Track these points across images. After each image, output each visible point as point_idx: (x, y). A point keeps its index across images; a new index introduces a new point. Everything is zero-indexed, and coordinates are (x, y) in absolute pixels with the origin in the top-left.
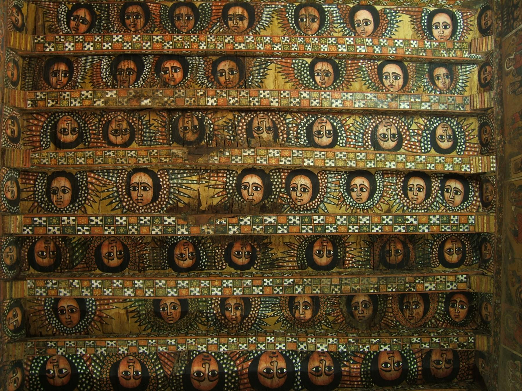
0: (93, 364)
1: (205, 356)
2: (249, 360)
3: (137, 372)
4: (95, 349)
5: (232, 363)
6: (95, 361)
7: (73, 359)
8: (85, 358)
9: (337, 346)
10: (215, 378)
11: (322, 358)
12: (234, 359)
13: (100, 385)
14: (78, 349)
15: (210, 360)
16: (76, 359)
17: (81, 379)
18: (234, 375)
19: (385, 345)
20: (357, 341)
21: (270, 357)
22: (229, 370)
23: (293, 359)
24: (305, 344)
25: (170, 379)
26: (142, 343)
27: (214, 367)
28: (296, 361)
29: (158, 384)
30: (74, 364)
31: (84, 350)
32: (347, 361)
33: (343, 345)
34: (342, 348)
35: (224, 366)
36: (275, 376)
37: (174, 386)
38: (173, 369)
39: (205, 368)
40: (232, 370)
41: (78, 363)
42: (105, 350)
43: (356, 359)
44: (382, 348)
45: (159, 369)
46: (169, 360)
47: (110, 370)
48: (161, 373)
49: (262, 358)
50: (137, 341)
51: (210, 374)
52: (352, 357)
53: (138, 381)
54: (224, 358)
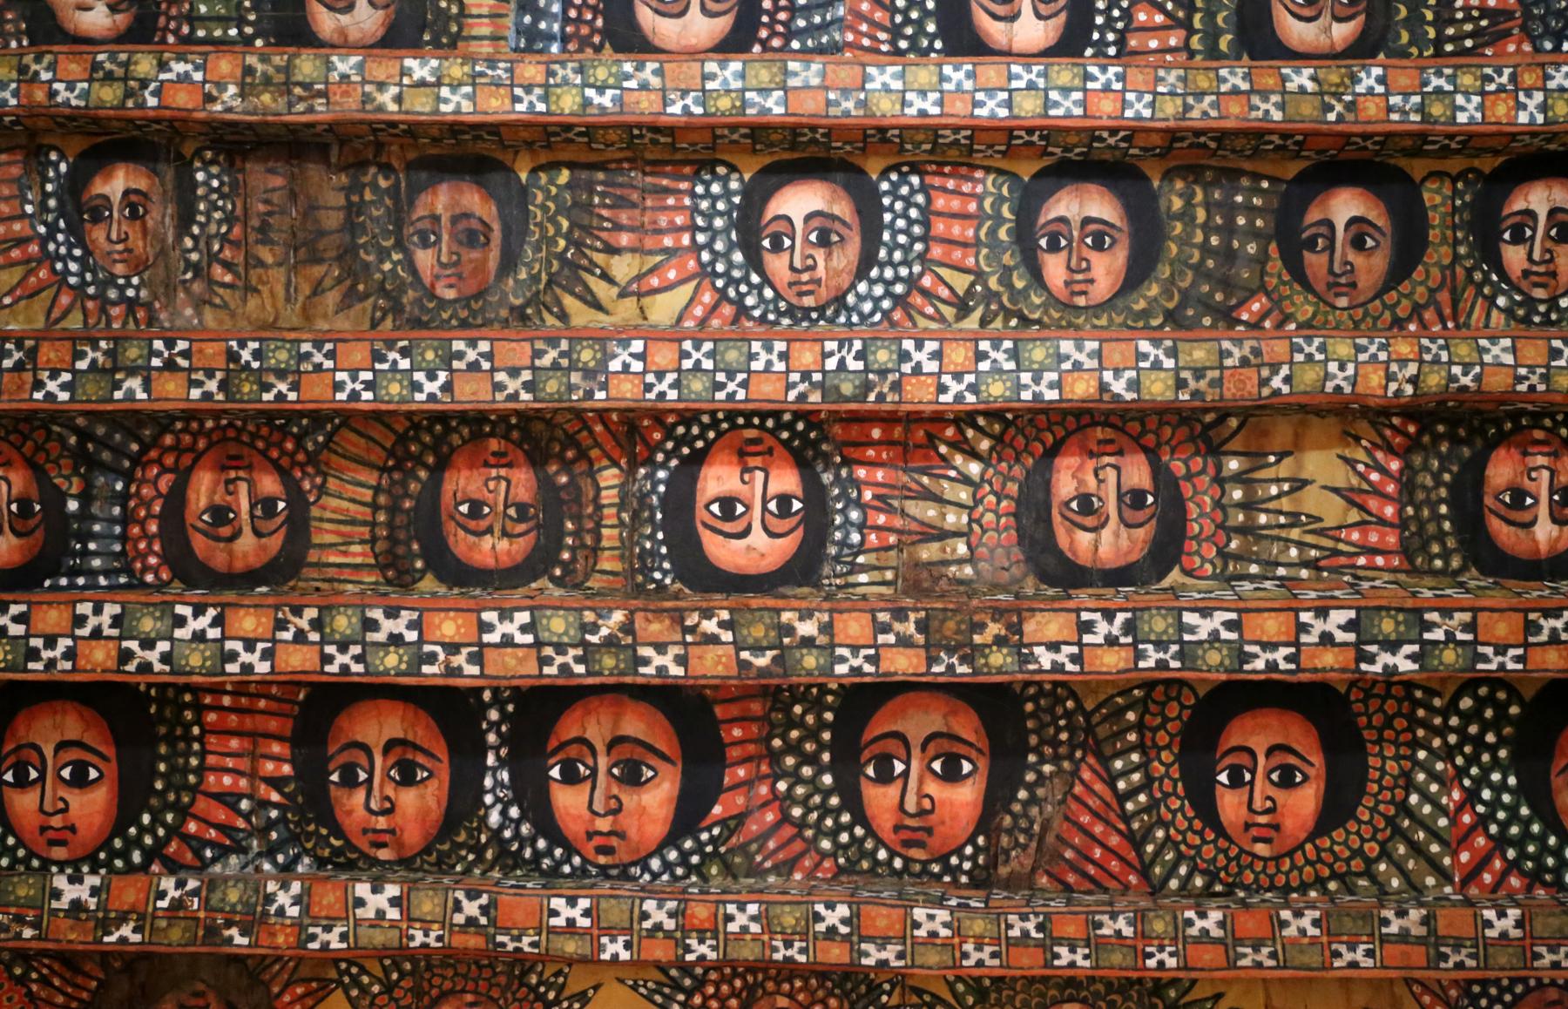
0: (1443, 822)
1: (920, 844)
2: (722, 822)
3: (1236, 781)
4: (1432, 932)
5: (797, 812)
6: (1435, 834)
7: (1541, 839)
8: (1481, 841)
9: (306, 911)
10: (876, 749)
11: (382, 823)
12: (788, 831)
13: (1414, 722)
14: (1515, 933)
15: (898, 828)
16: (1526, 835)
17: (1502, 741)
18: (790, 761)
19: (77, 905)
20: (212, 932)
21: (621, 835)
22: (813, 782)
23: (518, 822)
24: (459, 919)
25: (1083, 746)
26: (1209, 956)
27: (880, 799)
28: (504, 813)
29: (1139, 726)
30: (1537, 813)
31: (1488, 924)
32: (266, 804)
33: (281, 912)
34: (283, 899)
35: (834, 801)
36: (600, 747)
37: (1068, 715)
38: (1069, 792)
39: (922, 795)
40: (798, 780)
41: (1513, 815)
42: (1386, 922)
43: (221, 815)
44: (94, 891)
45: (1132, 793)
46: (1085, 831)
47: (1361, 791)
48: (1125, 773)
49: (657, 829)
50: (1232, 965)
51: (899, 767)
52: (241, 823)
53: (1234, 741)
54: (834, 834)
